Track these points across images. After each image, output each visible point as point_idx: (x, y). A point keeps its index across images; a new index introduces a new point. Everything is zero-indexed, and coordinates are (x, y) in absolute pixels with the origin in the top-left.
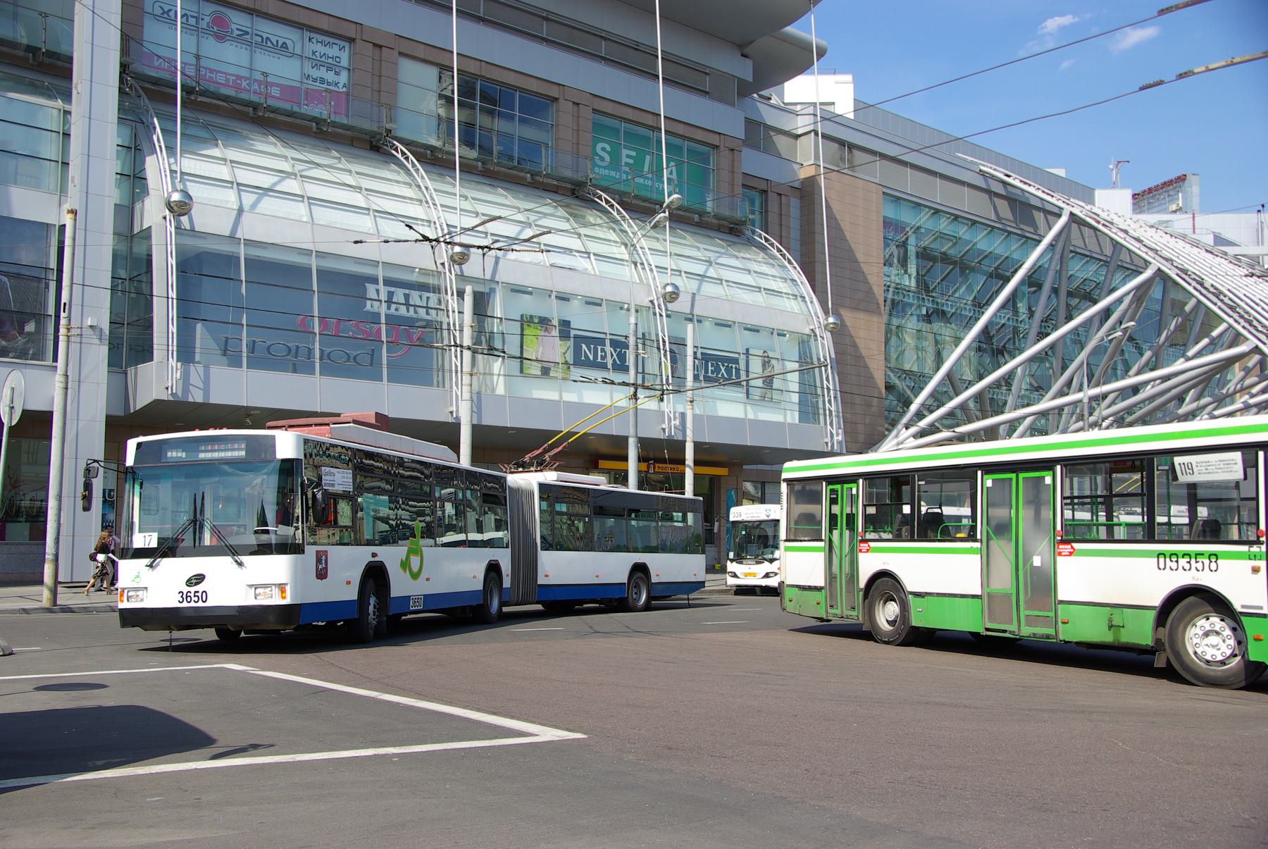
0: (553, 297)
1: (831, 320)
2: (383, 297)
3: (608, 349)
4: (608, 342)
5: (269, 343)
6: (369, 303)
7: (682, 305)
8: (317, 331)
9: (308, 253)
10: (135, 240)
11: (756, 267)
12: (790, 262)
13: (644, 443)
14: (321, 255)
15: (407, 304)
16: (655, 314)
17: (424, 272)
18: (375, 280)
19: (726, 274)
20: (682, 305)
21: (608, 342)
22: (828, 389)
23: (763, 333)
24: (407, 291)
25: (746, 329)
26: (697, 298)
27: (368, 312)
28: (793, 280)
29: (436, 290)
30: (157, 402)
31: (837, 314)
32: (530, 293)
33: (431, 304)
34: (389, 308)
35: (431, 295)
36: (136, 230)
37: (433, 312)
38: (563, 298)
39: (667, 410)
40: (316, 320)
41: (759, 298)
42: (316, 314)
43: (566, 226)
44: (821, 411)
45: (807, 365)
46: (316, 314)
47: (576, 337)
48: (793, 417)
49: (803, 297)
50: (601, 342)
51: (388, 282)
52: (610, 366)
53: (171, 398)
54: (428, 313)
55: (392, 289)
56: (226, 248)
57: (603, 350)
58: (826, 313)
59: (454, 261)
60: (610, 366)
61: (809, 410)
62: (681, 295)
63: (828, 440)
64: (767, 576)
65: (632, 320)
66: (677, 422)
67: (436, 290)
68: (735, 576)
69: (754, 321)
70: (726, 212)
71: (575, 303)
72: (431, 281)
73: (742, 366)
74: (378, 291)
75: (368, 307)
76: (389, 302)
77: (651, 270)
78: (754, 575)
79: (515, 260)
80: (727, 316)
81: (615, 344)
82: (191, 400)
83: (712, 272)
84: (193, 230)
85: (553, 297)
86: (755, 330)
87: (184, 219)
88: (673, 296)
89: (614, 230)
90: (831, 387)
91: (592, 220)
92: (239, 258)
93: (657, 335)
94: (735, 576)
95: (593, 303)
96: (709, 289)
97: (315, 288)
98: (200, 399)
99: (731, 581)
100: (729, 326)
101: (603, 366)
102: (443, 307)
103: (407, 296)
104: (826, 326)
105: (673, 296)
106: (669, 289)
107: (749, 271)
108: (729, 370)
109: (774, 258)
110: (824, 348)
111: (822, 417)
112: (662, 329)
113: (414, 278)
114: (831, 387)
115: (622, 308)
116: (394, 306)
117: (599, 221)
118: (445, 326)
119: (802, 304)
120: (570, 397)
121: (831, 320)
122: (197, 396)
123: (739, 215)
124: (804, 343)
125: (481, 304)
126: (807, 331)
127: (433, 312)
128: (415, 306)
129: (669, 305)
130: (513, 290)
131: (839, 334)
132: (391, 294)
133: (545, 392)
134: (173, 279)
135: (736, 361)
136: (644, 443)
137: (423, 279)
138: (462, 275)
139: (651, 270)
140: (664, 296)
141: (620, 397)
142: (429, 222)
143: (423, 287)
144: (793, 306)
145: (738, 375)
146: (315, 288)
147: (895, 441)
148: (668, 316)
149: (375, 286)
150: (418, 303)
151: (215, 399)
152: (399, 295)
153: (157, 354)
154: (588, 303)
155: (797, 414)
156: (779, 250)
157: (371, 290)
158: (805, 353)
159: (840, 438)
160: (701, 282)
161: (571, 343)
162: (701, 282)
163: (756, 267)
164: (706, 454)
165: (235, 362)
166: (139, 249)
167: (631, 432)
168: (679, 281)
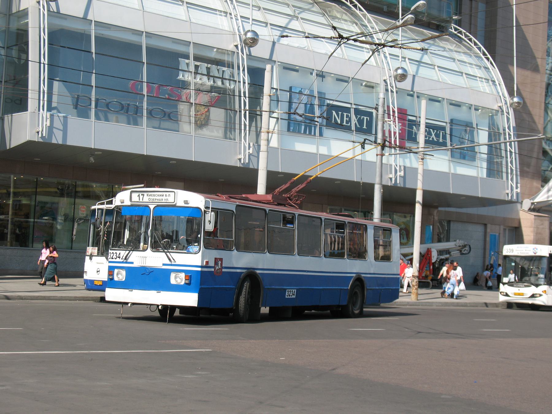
0: (314, 74)
1: (516, 100)
2: (192, 69)
3: (353, 117)
4: (352, 111)
5: (108, 101)
6: (181, 74)
7: (406, 85)
8: (145, 92)
9: (139, 33)
10: (11, 17)
11: (457, 56)
12: (484, 54)
13: (385, 188)
14: (149, 35)
15: (208, 75)
16: (387, 90)
17: (220, 51)
18: (187, 57)
19: (439, 62)
20: (406, 85)
21: (352, 111)
22: (511, 152)
23: (464, 108)
24: (209, 65)
25: (451, 104)
26: (417, 79)
27: (180, 81)
28: (486, 68)
29: (230, 65)
30: (29, 144)
31: (519, 94)
32: (297, 71)
33: (227, 76)
34: (195, 78)
35: (225, 69)
36: (14, 10)
37: (227, 83)
38: (321, 75)
39: (393, 164)
40: (145, 85)
41: (462, 81)
42: (145, 79)
43: (322, 20)
44: (504, 170)
45: (494, 134)
46: (145, 79)
47: (328, 105)
48: (484, 173)
49: (494, 82)
50: (348, 110)
51: (196, 58)
52: (353, 128)
53: (41, 140)
54: (223, 83)
55: (198, 63)
56: (78, 27)
57: (347, 116)
58: (511, 94)
59: (246, 44)
60: (353, 128)
61: (494, 170)
62: (409, 76)
63: (509, 191)
64: (533, 296)
65: (382, 96)
66: (402, 174)
67: (230, 65)
68: (507, 295)
69: (458, 98)
70: (435, 12)
71: (329, 80)
72: (226, 58)
73: (448, 131)
74: (188, 64)
75: (180, 77)
76: (196, 73)
77: (386, 57)
78: (522, 294)
79: (287, 45)
80: (439, 94)
81: (358, 112)
82: (54, 141)
83: (426, 59)
84: (58, 12)
85: (314, 74)
86: (457, 105)
87: (53, 4)
88: (403, 77)
89: (357, 24)
90: (513, 151)
91: (339, 15)
92: (90, 36)
93: (388, 107)
94: (507, 295)
95: (341, 80)
96: (424, 72)
97: (144, 60)
98: (60, 142)
99: (502, 298)
100: (439, 101)
101: (348, 129)
102: (236, 78)
103: (208, 69)
104: (511, 105)
105: (403, 77)
106: (400, 72)
107: (454, 59)
108: (437, 136)
109: (470, 49)
110: (507, 122)
111: (504, 175)
112: (394, 104)
113: (213, 55)
114: (513, 151)
115: (362, 85)
116: (199, 77)
117: (345, 17)
118: (237, 93)
119: (493, 87)
120: (323, 150)
121: (516, 100)
122: (57, 139)
123: (444, 16)
124: (492, 117)
125: (256, 75)
126: (496, 107)
127: (227, 83)
128: (214, 77)
129: (401, 85)
130: (285, 68)
131: (522, 113)
132: (197, 67)
133: (304, 145)
134: (45, 49)
135: (443, 128)
136: (385, 188)
137: (219, 57)
138: (250, 55)
139: (386, 57)
140: (396, 77)
141: (371, 154)
142: (226, 13)
143: (218, 63)
144: (485, 87)
145: (444, 137)
146: (144, 60)
147: (546, 196)
148: (397, 92)
149: (187, 61)
150: (217, 75)
151: (70, 142)
152: (203, 67)
153: (32, 103)
154: (338, 80)
155: (485, 171)
156: (475, 44)
157: (183, 62)
158: (493, 124)
159: (519, 190)
160: (419, 66)
161: (325, 108)
162: (419, 66)
163: (457, 56)
164: (433, 201)
165: (83, 113)
166: (14, 26)
167: (377, 180)
168: (404, 65)
